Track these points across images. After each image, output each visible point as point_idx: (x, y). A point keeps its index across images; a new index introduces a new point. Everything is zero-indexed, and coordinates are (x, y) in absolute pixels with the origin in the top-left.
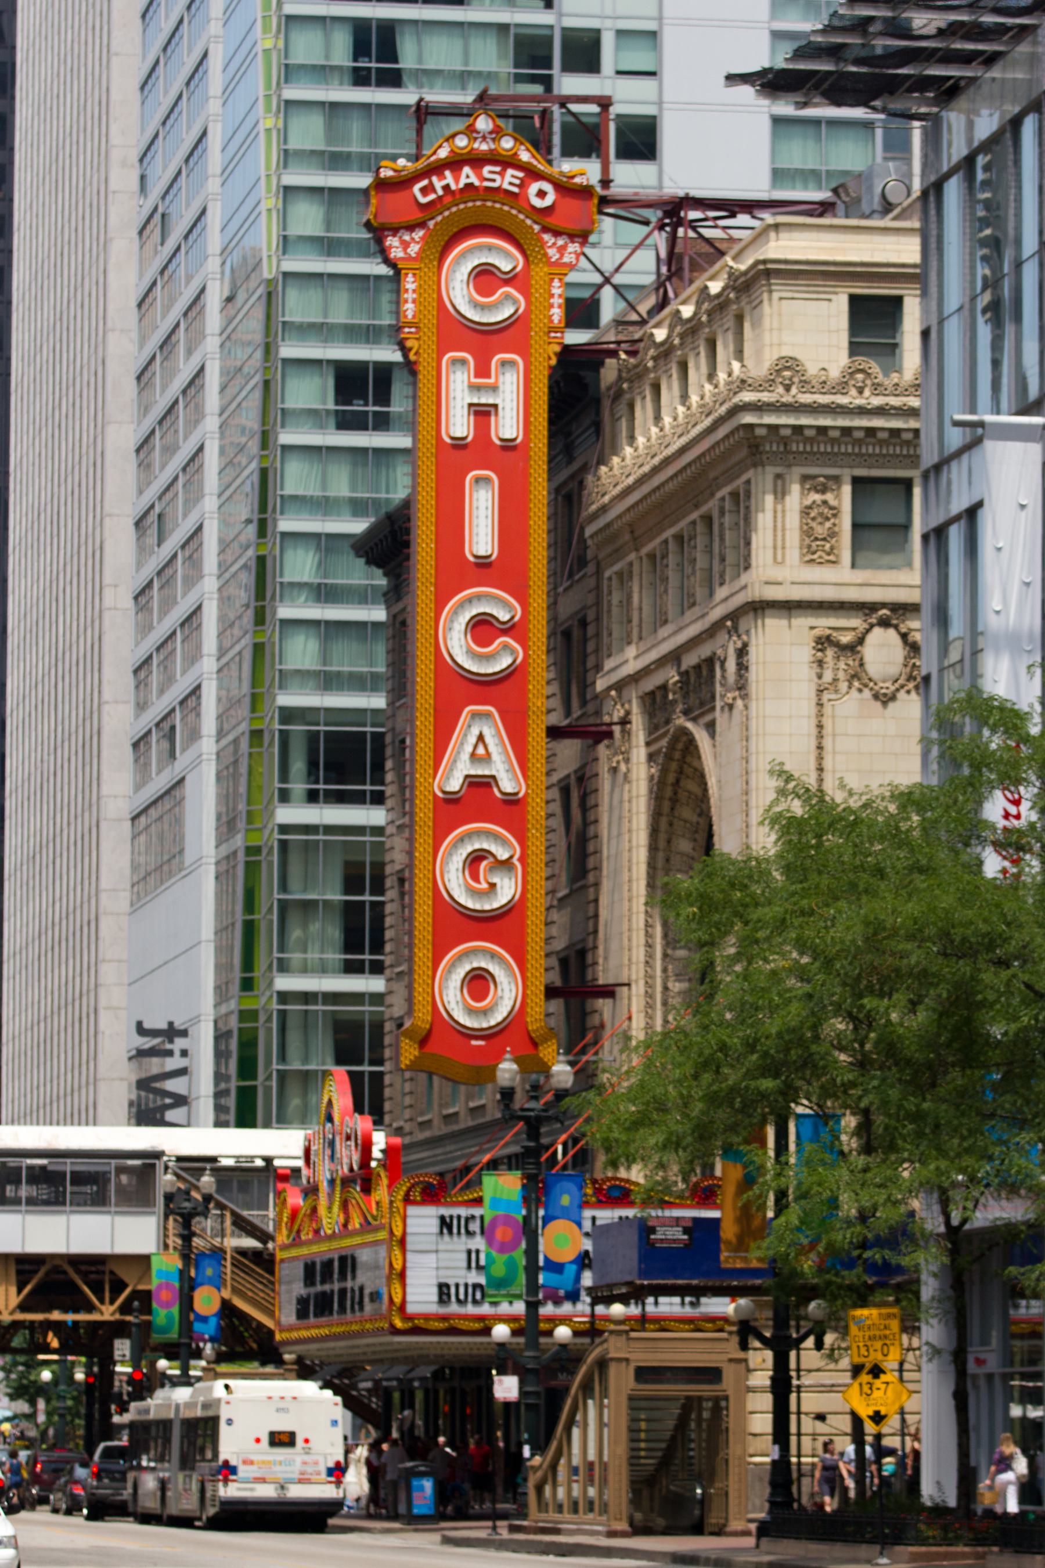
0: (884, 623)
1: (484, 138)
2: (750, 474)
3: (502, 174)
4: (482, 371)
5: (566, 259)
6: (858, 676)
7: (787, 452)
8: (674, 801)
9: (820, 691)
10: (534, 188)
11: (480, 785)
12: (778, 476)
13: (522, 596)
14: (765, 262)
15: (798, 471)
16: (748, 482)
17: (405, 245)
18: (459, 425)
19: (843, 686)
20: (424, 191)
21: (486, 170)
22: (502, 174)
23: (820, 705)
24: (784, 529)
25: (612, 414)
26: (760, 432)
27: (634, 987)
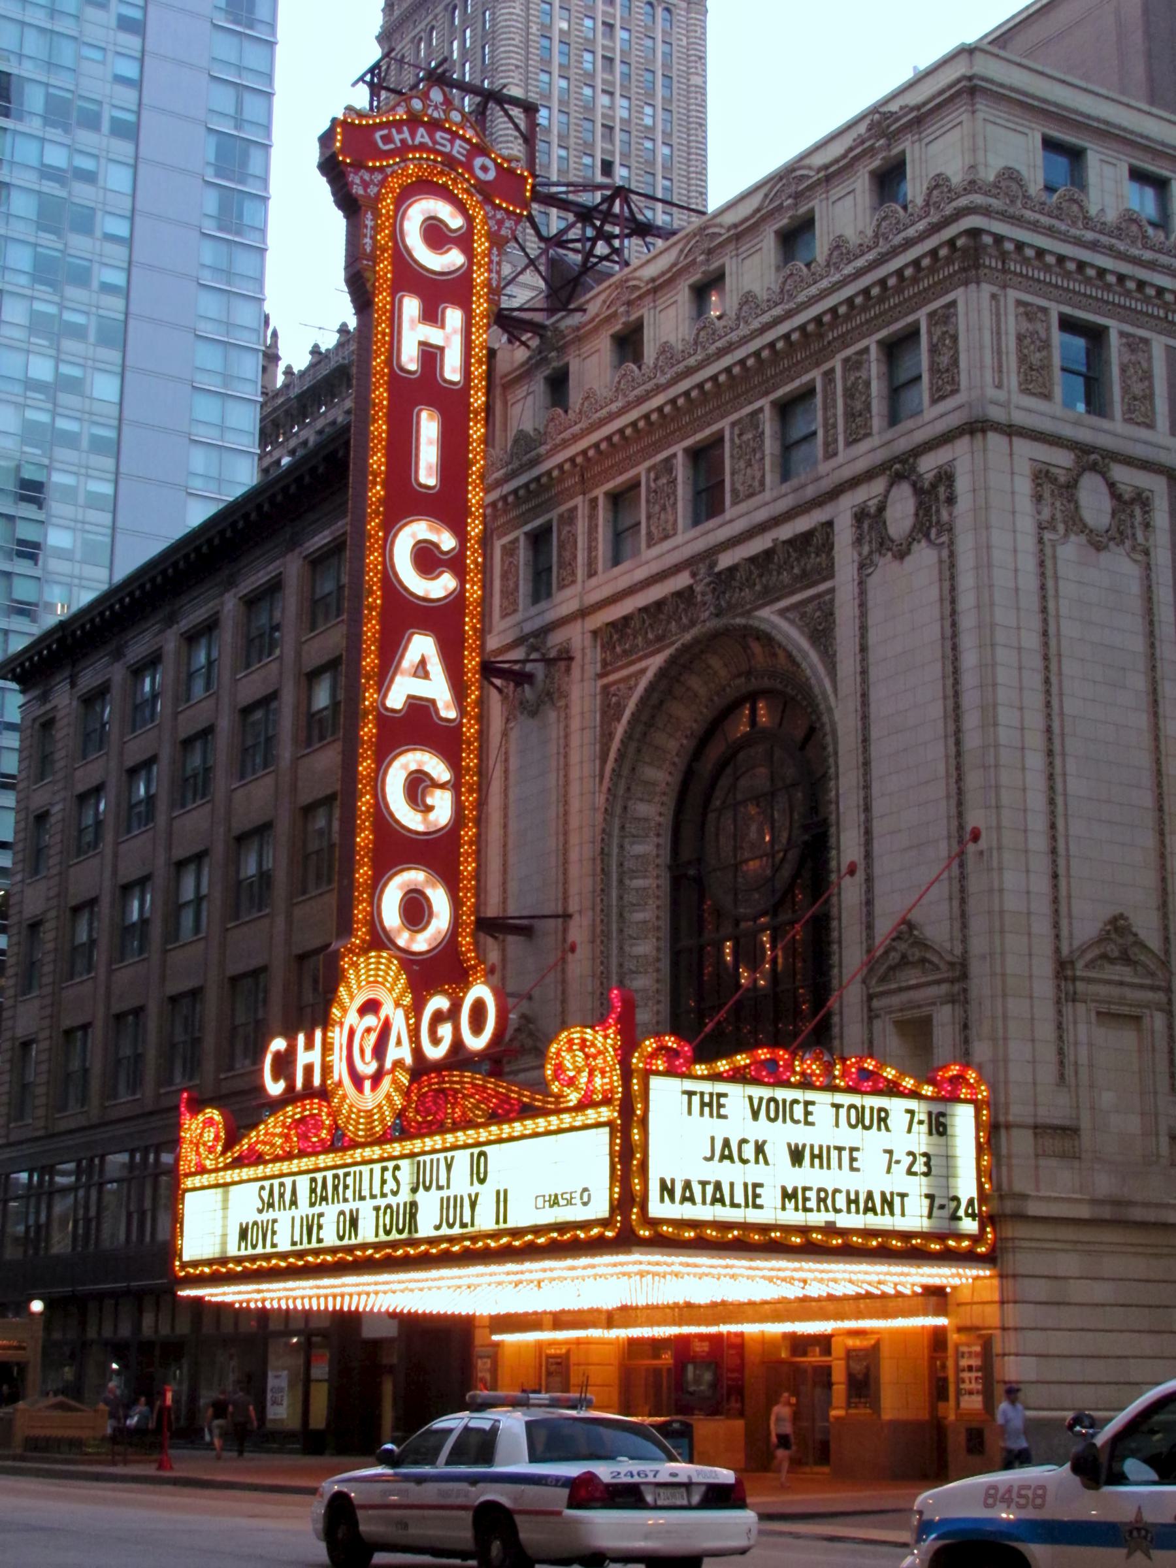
0: (1093, 467)
1: (436, 107)
2: (958, 294)
3: (452, 142)
4: (431, 316)
5: (503, 232)
6: (1075, 522)
7: (1004, 271)
8: (650, 724)
9: (1041, 527)
10: (478, 161)
11: (420, 708)
12: (994, 296)
13: (460, 533)
14: (970, 78)
15: (1013, 294)
16: (953, 304)
17: (365, 185)
18: (410, 358)
19: (1061, 528)
20: (387, 139)
21: (439, 135)
22: (452, 142)
23: (1041, 541)
24: (999, 353)
25: (505, 403)
26: (987, 240)
27: (576, 917)
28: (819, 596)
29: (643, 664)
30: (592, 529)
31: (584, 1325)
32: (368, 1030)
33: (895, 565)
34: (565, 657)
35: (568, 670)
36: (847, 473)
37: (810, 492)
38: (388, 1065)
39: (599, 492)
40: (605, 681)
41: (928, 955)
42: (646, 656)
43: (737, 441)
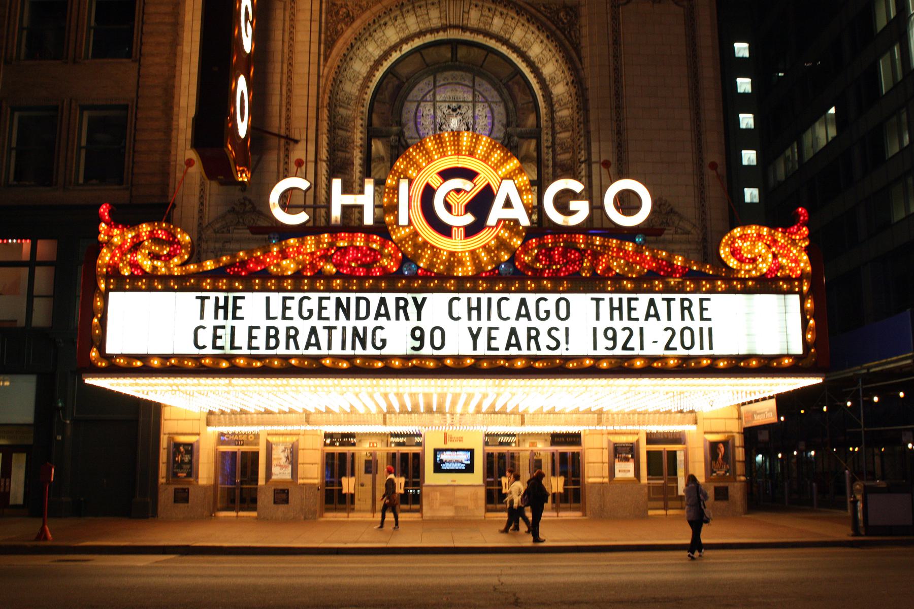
32: (458, 191)
38: (491, 220)
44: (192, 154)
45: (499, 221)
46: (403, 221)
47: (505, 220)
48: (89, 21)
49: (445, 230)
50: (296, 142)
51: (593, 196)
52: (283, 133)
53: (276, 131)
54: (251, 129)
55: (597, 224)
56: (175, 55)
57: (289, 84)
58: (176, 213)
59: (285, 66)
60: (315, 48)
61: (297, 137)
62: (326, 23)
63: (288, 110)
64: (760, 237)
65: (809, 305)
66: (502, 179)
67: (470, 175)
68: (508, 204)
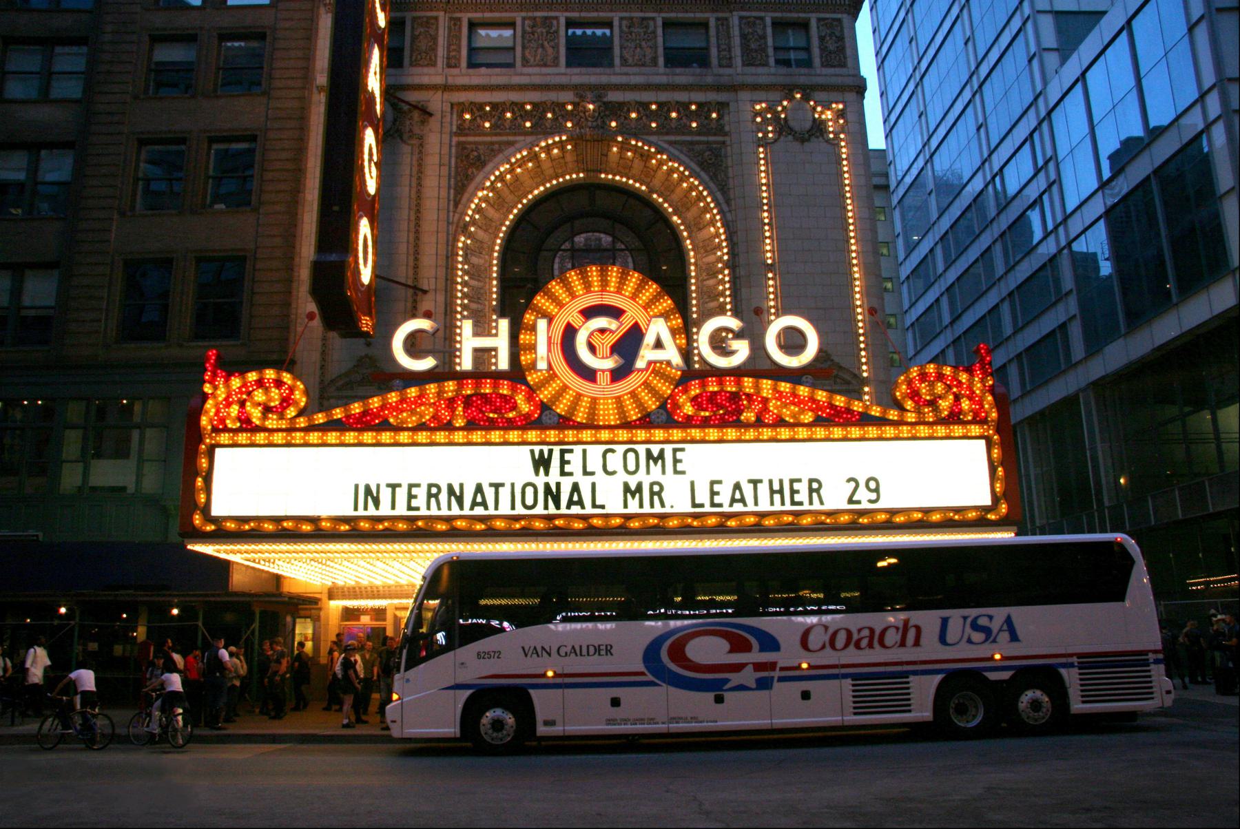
28: (708, 143)
29: (511, 138)
30: (453, 37)
31: (356, 597)
32: (602, 331)
33: (797, 145)
34: (426, 113)
35: (423, 122)
36: (749, 80)
37: (709, 80)
38: (640, 364)
39: (465, 17)
40: (463, 139)
41: (841, 374)
42: (515, 134)
43: (625, 28)
44: (312, 307)
45: (650, 363)
46: (542, 365)
47: (655, 362)
48: (207, 168)
49: (589, 374)
50: (425, 292)
51: (753, 333)
52: (410, 283)
53: (403, 281)
54: (376, 275)
55: (760, 367)
56: (297, 202)
57: (417, 232)
58: (297, 367)
59: (412, 213)
60: (444, 193)
61: (425, 287)
62: (457, 167)
63: (416, 259)
64: (940, 377)
65: (996, 452)
66: (651, 317)
67: (616, 313)
68: (659, 345)
